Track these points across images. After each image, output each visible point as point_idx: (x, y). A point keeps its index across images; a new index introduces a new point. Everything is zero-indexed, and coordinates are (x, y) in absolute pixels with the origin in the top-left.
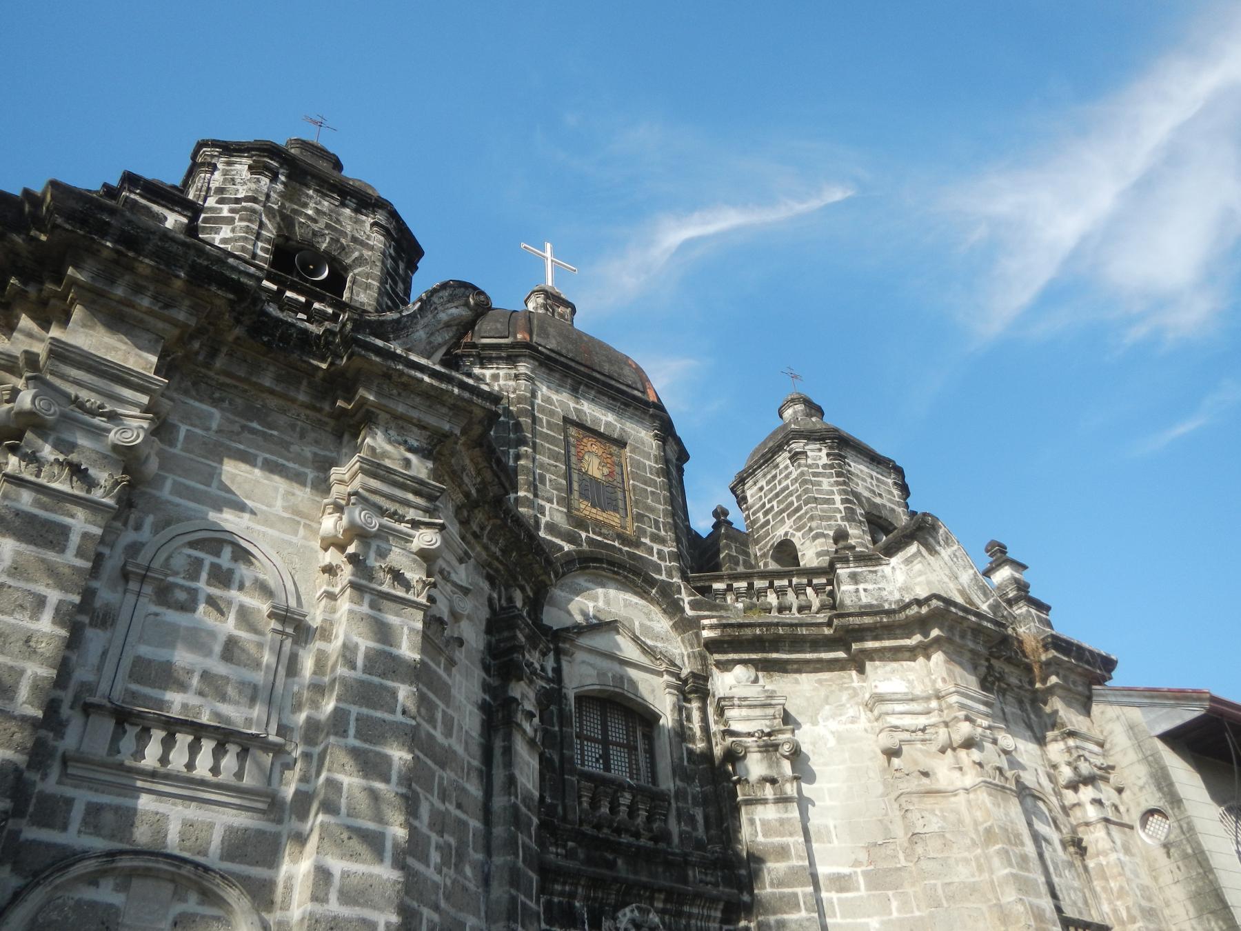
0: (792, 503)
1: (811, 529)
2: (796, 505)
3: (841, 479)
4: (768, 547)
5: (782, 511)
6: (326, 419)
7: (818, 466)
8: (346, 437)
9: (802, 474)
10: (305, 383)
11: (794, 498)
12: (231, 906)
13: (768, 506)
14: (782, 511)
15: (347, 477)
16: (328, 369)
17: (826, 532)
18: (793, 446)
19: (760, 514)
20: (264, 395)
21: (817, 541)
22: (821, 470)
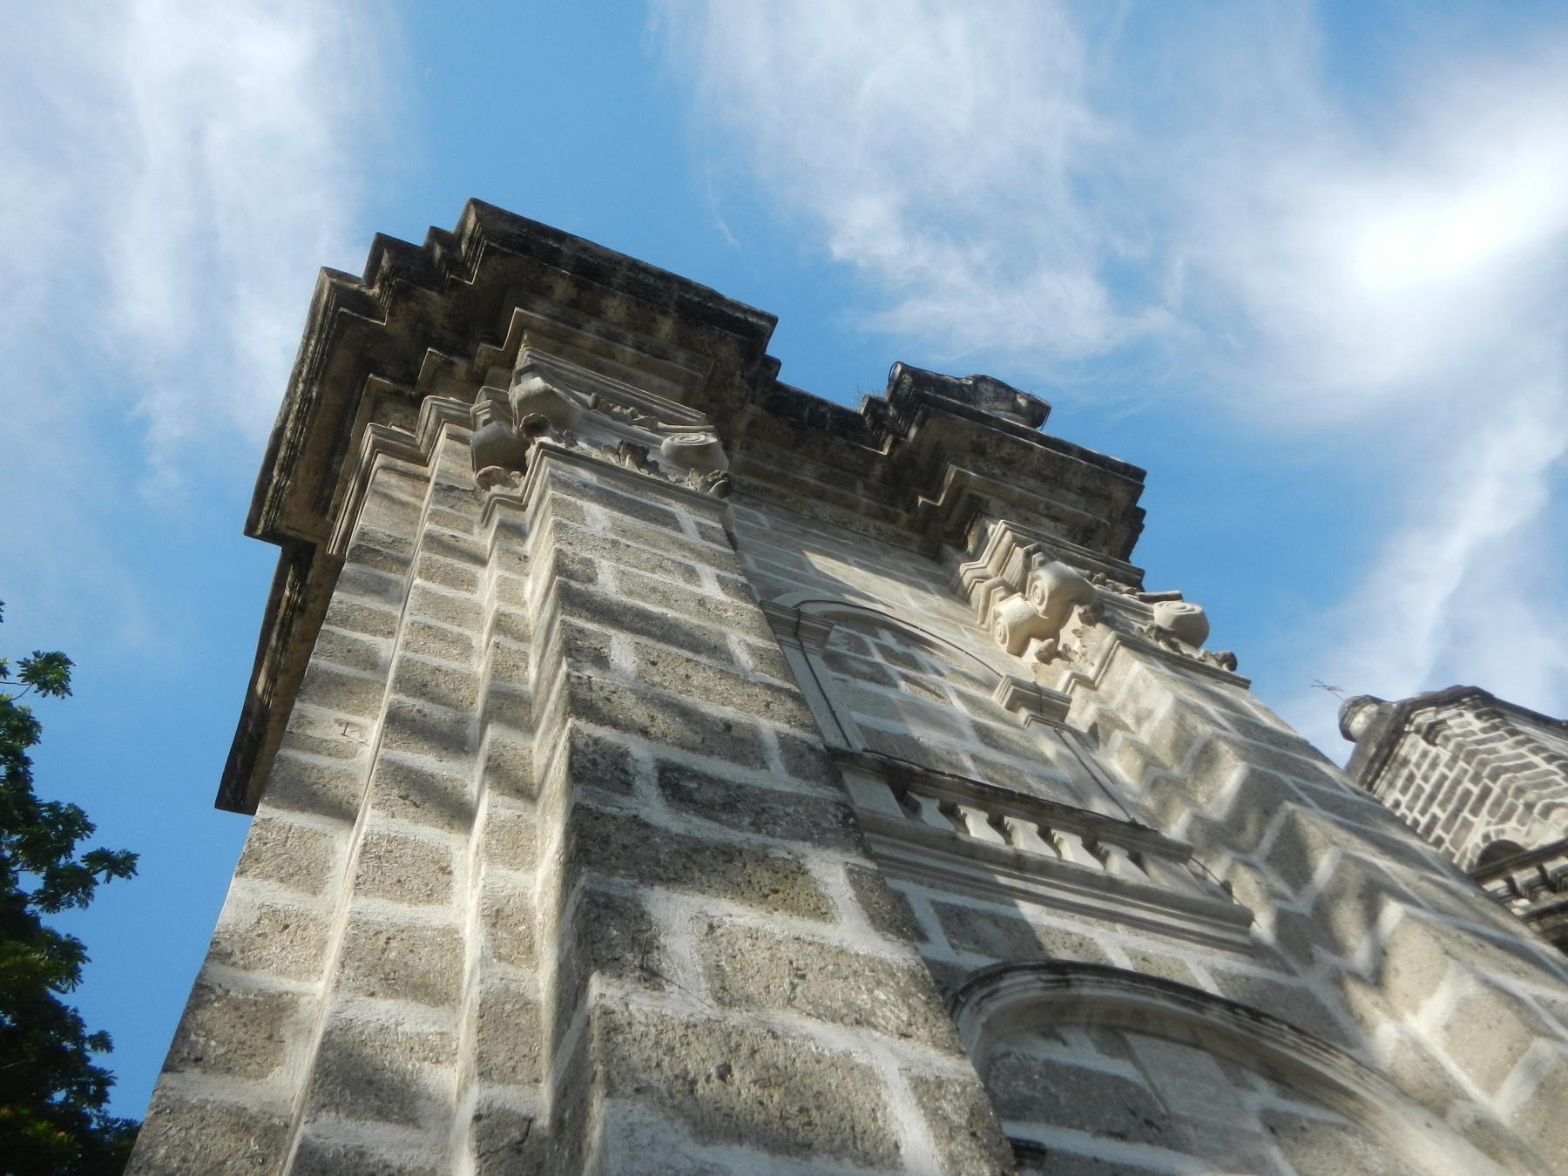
0: (1468, 793)
1: (1529, 807)
2: (1476, 790)
3: (1521, 737)
5: (1458, 811)
6: (905, 533)
7: (1473, 733)
8: (949, 550)
9: (1460, 746)
10: (859, 485)
11: (1467, 784)
12: (1350, 1095)
14: (1458, 811)
15: (990, 570)
16: (890, 453)
17: (1557, 801)
18: (1419, 720)
20: (813, 502)
21: (1555, 814)
22: (1482, 736)
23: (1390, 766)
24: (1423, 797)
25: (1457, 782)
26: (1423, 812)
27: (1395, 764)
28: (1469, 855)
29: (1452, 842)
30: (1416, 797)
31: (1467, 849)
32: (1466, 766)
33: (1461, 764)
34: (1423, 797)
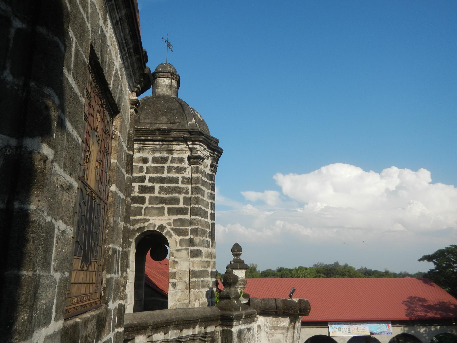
2: (181, 205)
4: (138, 226)
11: (181, 197)
13: (147, 184)
14: (163, 201)
18: (197, 147)
19: (136, 186)
22: (205, 179)
23: (163, 144)
24: (159, 175)
25: (179, 190)
26: (151, 180)
27: (166, 146)
28: (146, 224)
29: (146, 208)
30: (156, 170)
31: (149, 220)
32: (190, 191)
33: (189, 187)
34: (159, 175)
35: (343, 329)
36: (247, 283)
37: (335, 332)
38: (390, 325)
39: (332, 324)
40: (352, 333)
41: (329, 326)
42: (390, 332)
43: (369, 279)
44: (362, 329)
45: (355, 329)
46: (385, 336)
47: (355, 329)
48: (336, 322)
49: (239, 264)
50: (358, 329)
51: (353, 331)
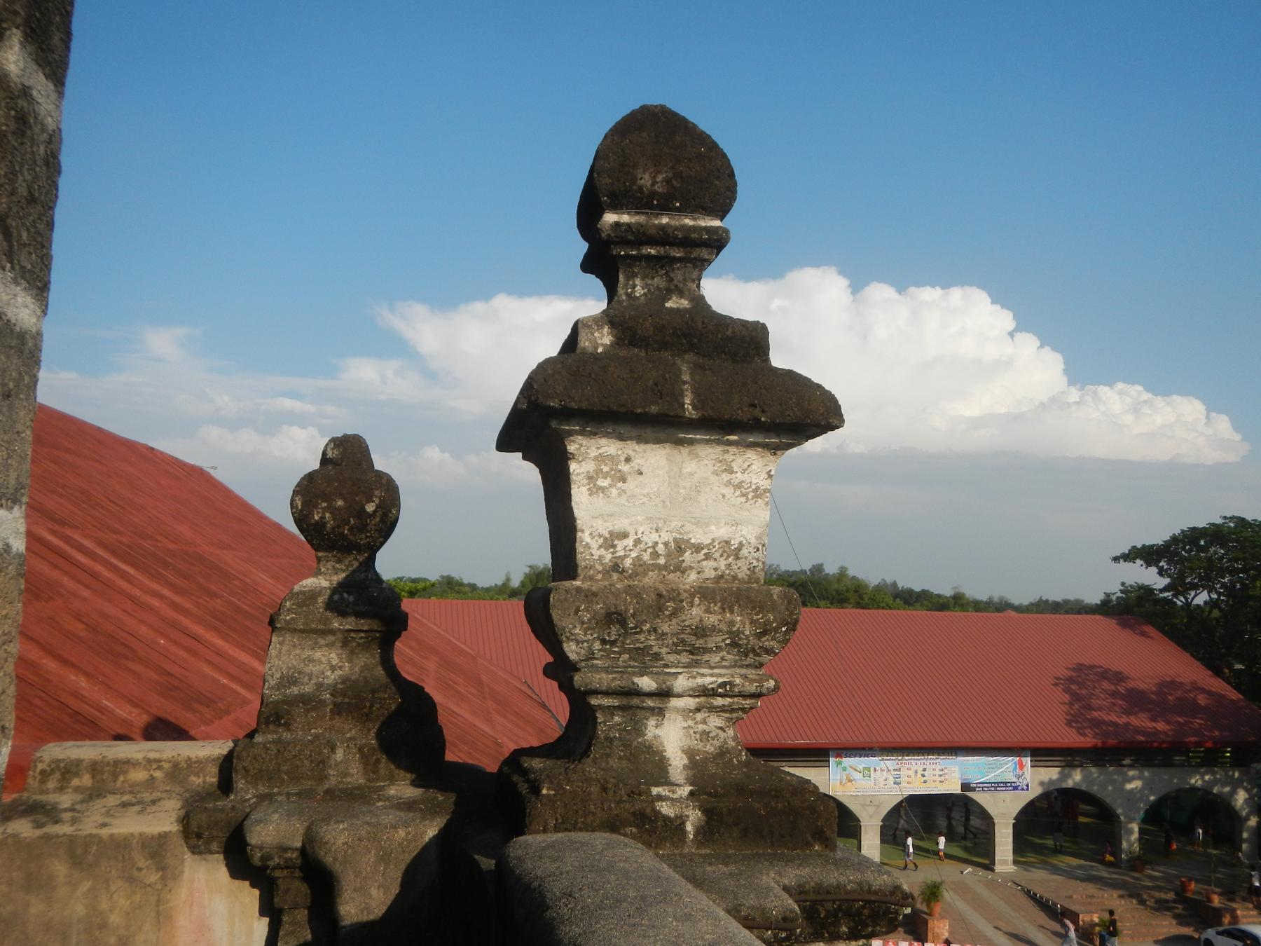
35: (878, 773)
36: (793, 626)
37: (850, 781)
38: (1027, 760)
39: (843, 755)
40: (907, 785)
41: (832, 760)
42: (1025, 782)
43: (979, 614)
44: (938, 773)
45: (916, 772)
46: (1008, 795)
47: (916, 772)
48: (857, 752)
49: (697, 367)
50: (926, 773)
51: (910, 779)
